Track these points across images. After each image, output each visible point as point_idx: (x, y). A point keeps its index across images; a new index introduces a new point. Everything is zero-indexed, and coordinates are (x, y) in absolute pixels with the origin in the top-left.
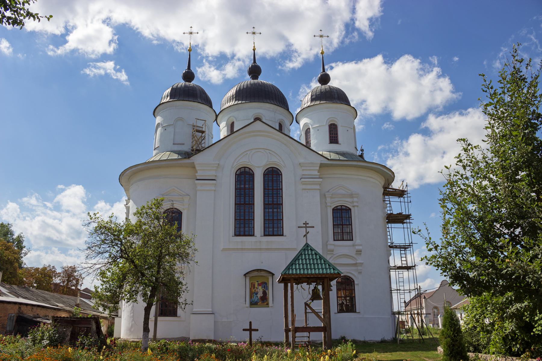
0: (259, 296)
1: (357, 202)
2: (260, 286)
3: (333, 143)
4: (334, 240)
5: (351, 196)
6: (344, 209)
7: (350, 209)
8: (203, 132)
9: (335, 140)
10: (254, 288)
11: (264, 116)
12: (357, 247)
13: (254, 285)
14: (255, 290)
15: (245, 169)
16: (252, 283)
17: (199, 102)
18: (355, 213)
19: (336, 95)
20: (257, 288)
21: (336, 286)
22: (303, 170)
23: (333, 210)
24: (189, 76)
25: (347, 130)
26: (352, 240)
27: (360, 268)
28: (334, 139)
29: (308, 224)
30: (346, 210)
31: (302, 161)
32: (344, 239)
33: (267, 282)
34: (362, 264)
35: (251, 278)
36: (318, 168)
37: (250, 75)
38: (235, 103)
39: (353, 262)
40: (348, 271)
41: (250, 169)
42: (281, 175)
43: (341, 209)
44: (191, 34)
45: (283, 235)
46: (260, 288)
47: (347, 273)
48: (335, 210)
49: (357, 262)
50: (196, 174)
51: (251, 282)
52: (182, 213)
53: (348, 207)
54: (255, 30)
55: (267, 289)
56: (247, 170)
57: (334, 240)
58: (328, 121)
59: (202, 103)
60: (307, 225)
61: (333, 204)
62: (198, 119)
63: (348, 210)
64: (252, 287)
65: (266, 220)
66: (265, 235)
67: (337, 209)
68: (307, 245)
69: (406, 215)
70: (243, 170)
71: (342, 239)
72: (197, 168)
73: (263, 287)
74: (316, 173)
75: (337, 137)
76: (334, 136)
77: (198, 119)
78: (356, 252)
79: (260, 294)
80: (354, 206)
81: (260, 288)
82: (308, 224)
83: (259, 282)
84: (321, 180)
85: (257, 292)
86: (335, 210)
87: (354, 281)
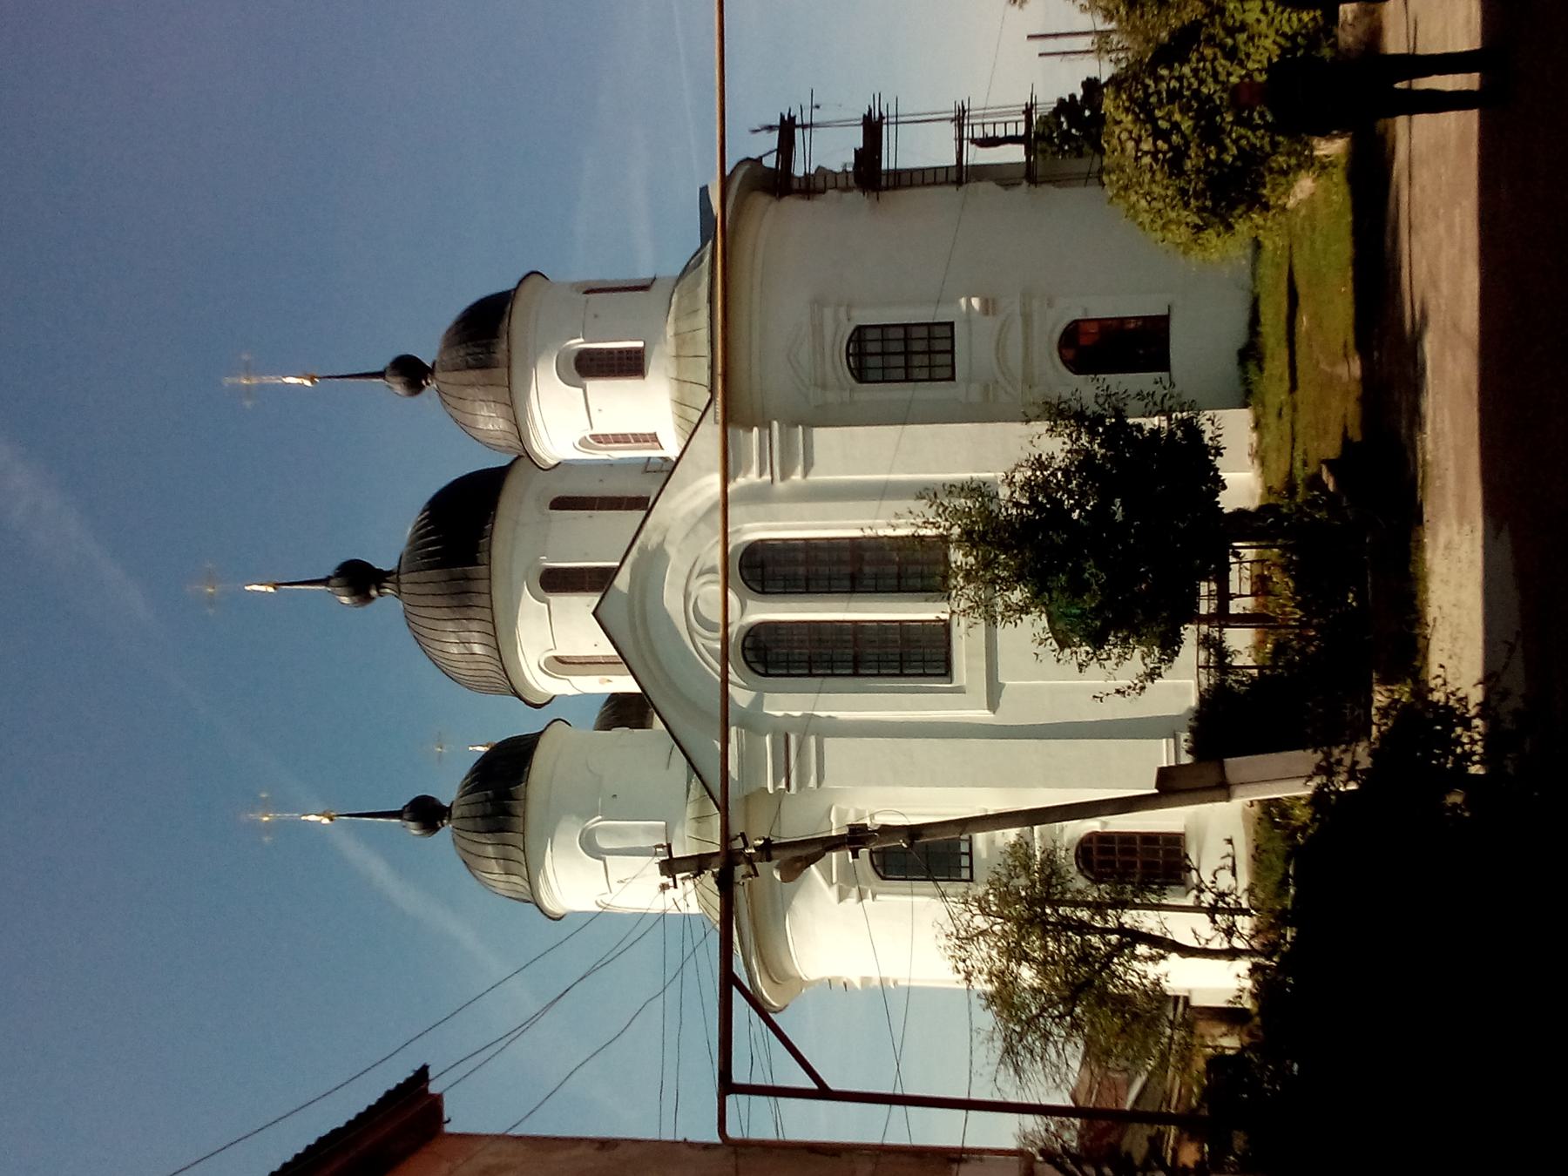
4: (952, 378)
7: (860, 330)
15: (749, 649)
26: (951, 324)
39: (1019, 321)
48: (860, 374)
53: (852, 334)
63: (859, 334)
65: (899, 586)
84: (775, 424)
86: (860, 374)
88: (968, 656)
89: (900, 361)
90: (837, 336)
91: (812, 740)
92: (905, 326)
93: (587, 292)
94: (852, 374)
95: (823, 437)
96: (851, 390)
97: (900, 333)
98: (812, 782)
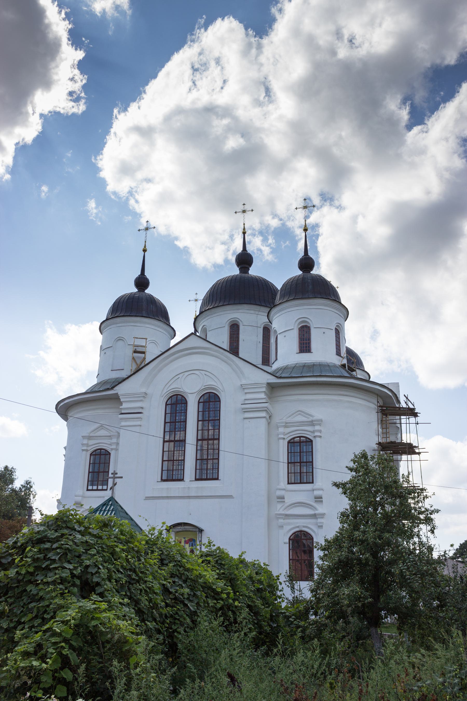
1: (320, 431)
2: (187, 543)
4: (288, 483)
5: (312, 423)
6: (303, 442)
7: (311, 441)
8: (144, 353)
9: (306, 347)
11: (241, 321)
12: (317, 493)
15: (177, 397)
18: (318, 445)
19: (310, 287)
21: (288, 545)
22: (246, 393)
23: (289, 442)
25: (324, 333)
26: (313, 483)
27: (319, 520)
29: (117, 474)
30: (306, 442)
31: (244, 382)
32: (302, 482)
34: (324, 514)
35: (177, 533)
36: (264, 390)
37: (238, 266)
40: (305, 525)
41: (182, 396)
42: (220, 401)
43: (300, 442)
44: (147, 230)
45: (217, 479)
47: (304, 527)
48: (291, 443)
49: (316, 512)
50: (120, 407)
52: (110, 454)
54: (246, 207)
56: (179, 397)
57: (288, 483)
59: (147, 317)
60: (116, 476)
62: (137, 338)
66: (196, 480)
67: (294, 442)
68: (112, 499)
69: (407, 443)
70: (174, 399)
71: (299, 482)
72: (122, 400)
73: (191, 545)
74: (263, 396)
75: (309, 343)
76: (305, 342)
77: (137, 338)
78: (316, 498)
80: (315, 437)
82: (117, 474)
83: (186, 539)
87: (313, 539)
88: (168, 489)
90: (307, 432)
91: (138, 423)
92: (312, 462)
93: (336, 329)
96: (284, 439)
98: (123, 424)
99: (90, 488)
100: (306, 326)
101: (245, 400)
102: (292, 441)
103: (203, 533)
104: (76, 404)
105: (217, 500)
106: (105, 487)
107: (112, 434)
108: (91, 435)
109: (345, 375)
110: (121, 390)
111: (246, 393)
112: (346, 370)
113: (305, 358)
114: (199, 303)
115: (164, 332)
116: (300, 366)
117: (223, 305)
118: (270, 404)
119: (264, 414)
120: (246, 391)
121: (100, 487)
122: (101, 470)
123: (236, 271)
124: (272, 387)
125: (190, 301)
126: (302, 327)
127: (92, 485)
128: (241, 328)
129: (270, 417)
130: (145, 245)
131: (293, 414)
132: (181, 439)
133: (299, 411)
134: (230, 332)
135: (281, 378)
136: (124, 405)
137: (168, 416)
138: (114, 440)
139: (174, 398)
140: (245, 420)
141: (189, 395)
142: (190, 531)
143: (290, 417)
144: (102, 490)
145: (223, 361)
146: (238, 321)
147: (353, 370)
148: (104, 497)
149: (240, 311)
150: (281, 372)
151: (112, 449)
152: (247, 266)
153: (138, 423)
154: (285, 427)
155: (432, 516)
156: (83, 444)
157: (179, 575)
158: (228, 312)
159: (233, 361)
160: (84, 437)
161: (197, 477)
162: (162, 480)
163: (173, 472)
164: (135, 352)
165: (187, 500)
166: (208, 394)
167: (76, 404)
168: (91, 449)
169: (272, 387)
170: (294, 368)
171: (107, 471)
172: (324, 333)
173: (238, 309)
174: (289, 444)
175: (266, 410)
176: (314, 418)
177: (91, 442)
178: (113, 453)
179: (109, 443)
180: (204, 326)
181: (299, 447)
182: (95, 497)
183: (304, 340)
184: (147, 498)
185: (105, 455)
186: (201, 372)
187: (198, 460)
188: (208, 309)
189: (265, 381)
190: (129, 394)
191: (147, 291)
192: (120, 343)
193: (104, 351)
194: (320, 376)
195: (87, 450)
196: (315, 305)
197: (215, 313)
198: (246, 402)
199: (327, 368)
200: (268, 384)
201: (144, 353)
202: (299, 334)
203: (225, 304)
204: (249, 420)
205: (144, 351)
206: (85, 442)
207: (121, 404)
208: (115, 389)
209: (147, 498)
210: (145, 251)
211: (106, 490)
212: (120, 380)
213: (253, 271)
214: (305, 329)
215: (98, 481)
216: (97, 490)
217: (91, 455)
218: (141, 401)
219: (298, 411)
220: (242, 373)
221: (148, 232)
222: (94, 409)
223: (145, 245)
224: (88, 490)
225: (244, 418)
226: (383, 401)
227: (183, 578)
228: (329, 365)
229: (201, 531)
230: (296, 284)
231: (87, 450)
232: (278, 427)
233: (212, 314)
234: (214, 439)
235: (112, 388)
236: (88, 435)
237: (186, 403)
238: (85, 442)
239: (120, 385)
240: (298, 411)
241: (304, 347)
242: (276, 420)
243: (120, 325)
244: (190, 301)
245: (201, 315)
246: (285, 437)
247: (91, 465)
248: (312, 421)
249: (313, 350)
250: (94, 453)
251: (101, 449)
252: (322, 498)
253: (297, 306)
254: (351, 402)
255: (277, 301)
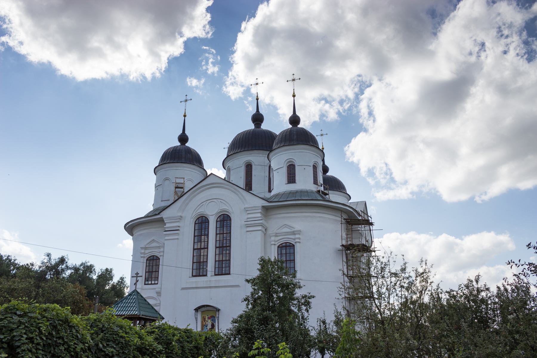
0: (208, 328)
1: (299, 238)
3: (291, 183)
5: (294, 233)
7: (294, 246)
8: (182, 188)
9: (292, 180)
10: (205, 321)
13: (205, 318)
14: (205, 323)
15: (202, 218)
16: (203, 317)
17: (182, 163)
18: (298, 248)
19: (295, 137)
20: (207, 321)
22: (248, 214)
23: (278, 247)
24: (183, 139)
25: (305, 169)
28: (291, 178)
29: (139, 274)
30: (290, 246)
31: (247, 206)
33: (215, 316)
35: (202, 312)
36: (260, 211)
37: (253, 123)
38: (236, 152)
41: (206, 217)
43: (286, 246)
45: (229, 274)
46: (209, 321)
48: (280, 247)
51: (203, 316)
52: (159, 259)
55: (215, 322)
58: (286, 162)
60: (138, 275)
61: (276, 243)
62: (177, 178)
64: (203, 320)
72: (165, 222)
74: (259, 215)
75: (295, 177)
76: (291, 176)
77: (177, 178)
79: (209, 326)
80: (296, 242)
81: (209, 321)
82: (139, 274)
83: (209, 316)
85: (207, 324)
86: (280, 247)
88: (196, 282)
89: (284, 258)
90: (290, 239)
91: (176, 237)
92: (294, 260)
93: (314, 166)
94: (280, 245)
95: (259, 236)
97: (292, 258)
98: (167, 238)
99: (147, 283)
100: (292, 165)
101: (248, 218)
102: (281, 246)
103: (220, 311)
104: (136, 225)
105: (229, 289)
106: (156, 282)
107: (161, 245)
108: (147, 246)
109: (319, 199)
110: (165, 215)
111: (248, 214)
112: (320, 195)
113: (292, 187)
114: (227, 150)
115: (198, 173)
116: (287, 193)
117: (244, 151)
118: (266, 221)
119: (260, 228)
120: (248, 212)
121: (153, 282)
122: (154, 270)
123: (252, 126)
124: (266, 209)
125: (224, 148)
126: (290, 165)
127: (148, 281)
128: (253, 167)
129: (266, 230)
130: (185, 112)
131: (281, 227)
132: (228, 245)
133: (285, 225)
134: (246, 170)
135: (271, 202)
136: (167, 225)
137: (196, 231)
138: (162, 250)
139: (200, 219)
140: (247, 232)
141: (210, 216)
142: (210, 310)
143: (278, 229)
144: (155, 284)
145: (233, 192)
146: (251, 163)
147: (326, 194)
148: (155, 289)
149: (253, 155)
150: (274, 198)
151: (161, 256)
152: (260, 123)
153: (176, 237)
154: (276, 236)
155: (310, 300)
156: (141, 253)
157: (113, 340)
158: (244, 156)
159: (239, 192)
160: (142, 248)
161: (216, 273)
162: (193, 276)
163: (200, 270)
164: (176, 188)
165: (209, 289)
166: (223, 215)
167: (136, 225)
168: (147, 256)
169: (266, 209)
170: (284, 194)
171: (158, 271)
172: (305, 169)
173: (251, 154)
174: (279, 248)
175: (261, 225)
176: (295, 230)
177: (147, 251)
178: (161, 258)
179: (158, 251)
180: (228, 166)
181: (285, 250)
182: (150, 289)
183: (290, 175)
184: (183, 289)
185: (156, 260)
186: (218, 200)
187: (217, 261)
188: (231, 155)
189: (261, 205)
190: (170, 218)
191: (187, 145)
192: (167, 182)
193: (157, 188)
194: (298, 200)
195: (144, 257)
196: (298, 149)
197: (235, 157)
198: (249, 220)
199: (306, 194)
200: (262, 206)
201: (182, 188)
202: (288, 170)
203: (242, 151)
204: (250, 232)
205: (183, 186)
206: (143, 251)
207: (165, 224)
208: (160, 214)
209: (183, 289)
210: (185, 116)
211: (157, 284)
212: (165, 207)
213: (264, 126)
214: (292, 166)
215: (152, 278)
216: (151, 284)
217: (147, 260)
218: (178, 221)
219: (284, 225)
220: (245, 200)
221: (187, 103)
222: (144, 229)
223: (185, 112)
224: (145, 284)
225: (247, 231)
226: (348, 215)
227: (117, 342)
228: (307, 192)
229: (219, 310)
230: (286, 136)
231: (144, 257)
232: (270, 237)
233: (233, 158)
234: (204, 248)
235: (159, 214)
236: (144, 246)
237: (208, 222)
238: (143, 251)
239: (164, 211)
240: (284, 225)
241: (291, 179)
242: (270, 232)
243: (167, 169)
244: (224, 148)
245: (228, 158)
246: (276, 243)
247: (147, 267)
248: (294, 232)
249: (296, 182)
250: (149, 259)
251: (153, 256)
252: (160, 293)
253: (286, 150)
254: (322, 217)
255: (274, 147)
